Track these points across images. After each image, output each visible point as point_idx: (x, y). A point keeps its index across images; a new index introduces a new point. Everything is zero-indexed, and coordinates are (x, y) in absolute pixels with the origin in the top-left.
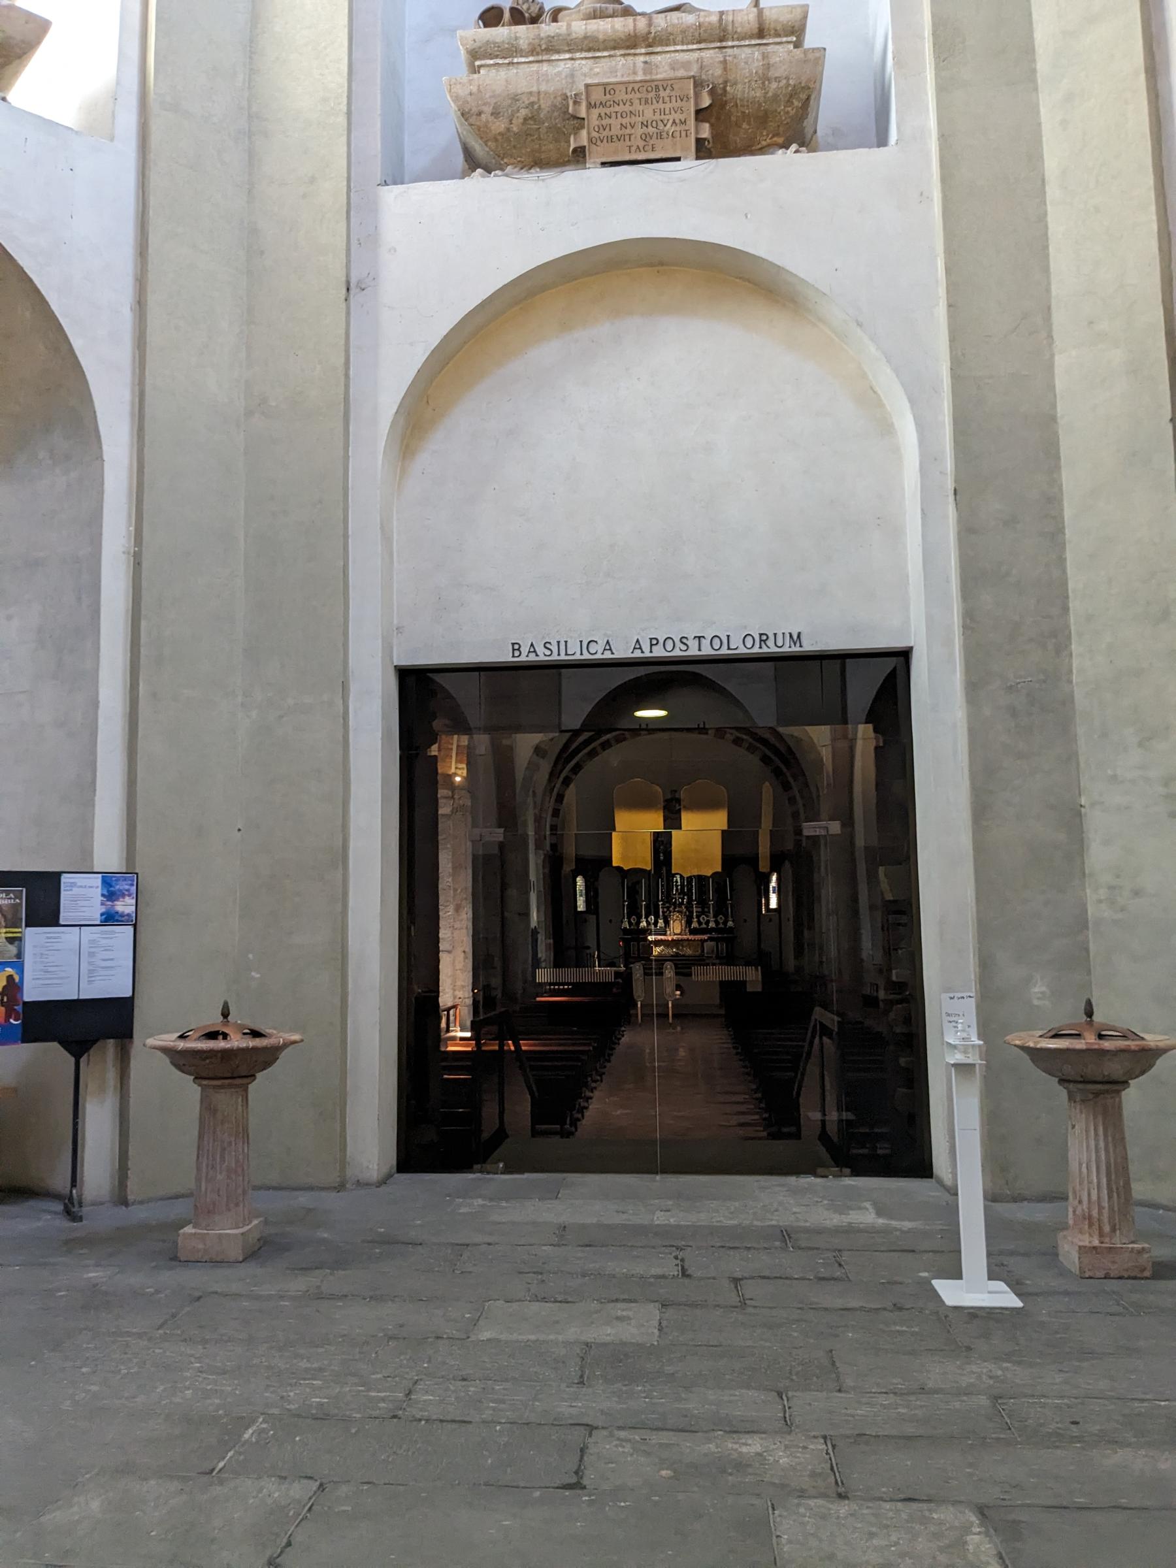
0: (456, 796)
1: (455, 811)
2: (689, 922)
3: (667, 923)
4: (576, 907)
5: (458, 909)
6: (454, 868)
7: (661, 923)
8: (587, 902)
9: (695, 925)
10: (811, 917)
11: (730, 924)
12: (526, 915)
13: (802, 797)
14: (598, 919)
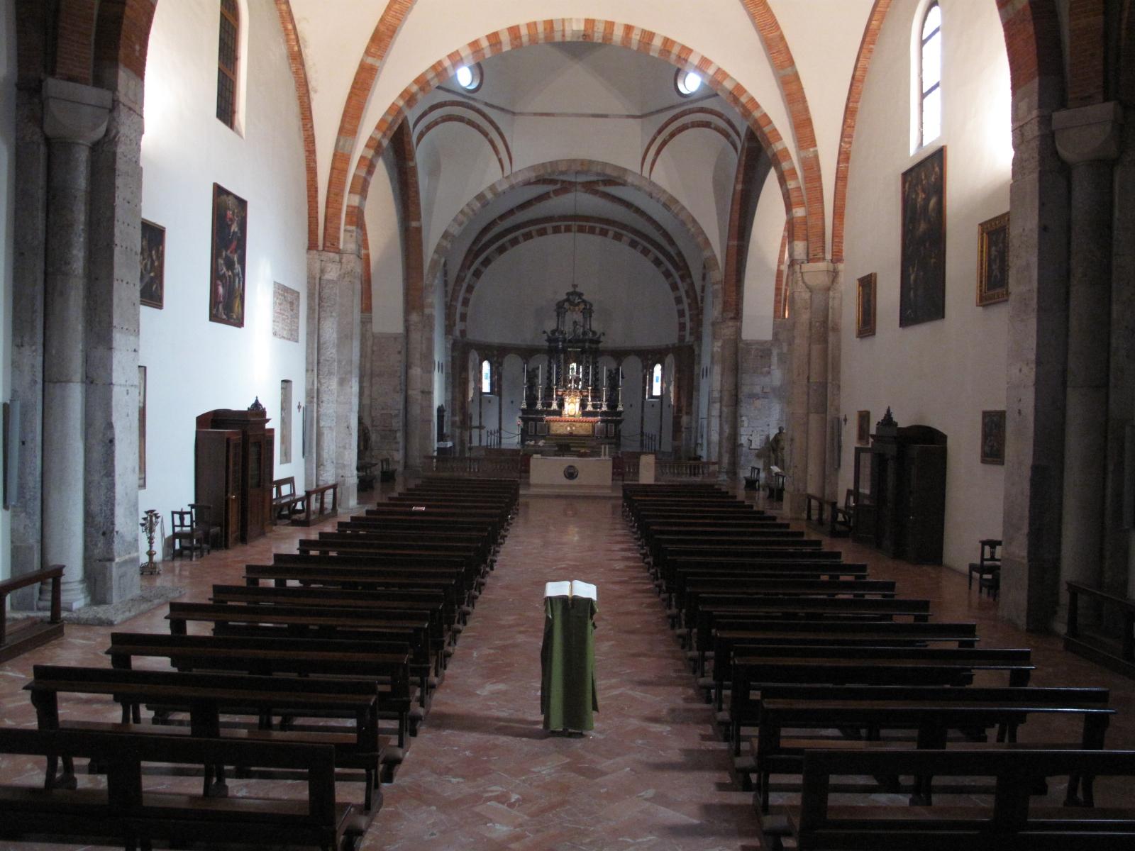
0: (344, 260)
1: (342, 277)
2: (583, 406)
3: (561, 405)
4: (481, 389)
5: (342, 382)
6: (340, 339)
7: (555, 406)
8: (492, 385)
9: (589, 408)
10: (690, 404)
11: (620, 408)
12: (428, 393)
13: (688, 296)
14: (500, 399)
